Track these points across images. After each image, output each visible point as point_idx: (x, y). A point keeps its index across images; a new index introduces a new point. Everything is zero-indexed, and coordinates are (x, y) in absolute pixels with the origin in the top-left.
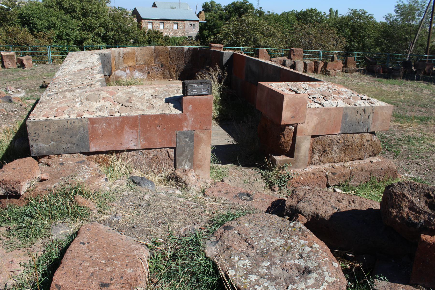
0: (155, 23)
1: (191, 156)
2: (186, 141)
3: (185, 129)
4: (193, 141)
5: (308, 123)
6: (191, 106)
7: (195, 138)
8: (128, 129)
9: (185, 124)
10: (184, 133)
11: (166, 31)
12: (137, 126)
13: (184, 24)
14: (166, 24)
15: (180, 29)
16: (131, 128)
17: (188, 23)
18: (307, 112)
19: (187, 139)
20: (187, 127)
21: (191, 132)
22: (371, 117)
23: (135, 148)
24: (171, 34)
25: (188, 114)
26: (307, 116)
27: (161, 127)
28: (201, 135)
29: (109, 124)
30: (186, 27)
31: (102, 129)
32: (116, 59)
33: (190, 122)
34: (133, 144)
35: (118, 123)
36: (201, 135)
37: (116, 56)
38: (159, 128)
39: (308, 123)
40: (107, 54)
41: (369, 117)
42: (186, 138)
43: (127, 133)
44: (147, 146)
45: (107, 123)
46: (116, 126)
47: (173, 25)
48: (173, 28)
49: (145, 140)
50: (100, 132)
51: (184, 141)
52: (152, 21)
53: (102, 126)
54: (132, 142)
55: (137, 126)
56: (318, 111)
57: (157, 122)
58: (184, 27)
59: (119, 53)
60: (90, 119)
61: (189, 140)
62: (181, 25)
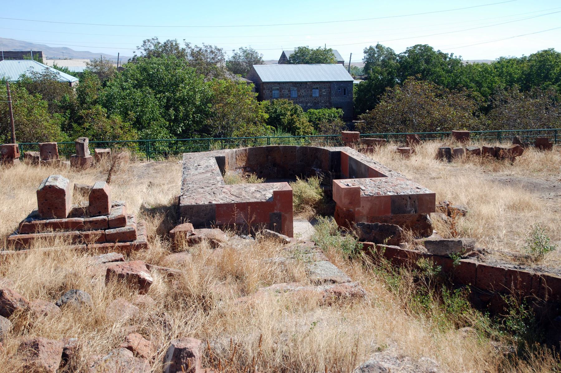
0: (283, 89)
3: (275, 211)
5: (363, 207)
9: (276, 208)
10: (275, 214)
14: (301, 89)
18: (362, 199)
19: (277, 218)
22: (416, 202)
25: (277, 202)
26: (361, 202)
28: (286, 215)
30: (332, 92)
36: (286, 215)
39: (363, 207)
41: (414, 202)
42: (276, 217)
47: (311, 91)
48: (311, 96)
56: (370, 199)
58: (330, 93)
62: (324, 90)
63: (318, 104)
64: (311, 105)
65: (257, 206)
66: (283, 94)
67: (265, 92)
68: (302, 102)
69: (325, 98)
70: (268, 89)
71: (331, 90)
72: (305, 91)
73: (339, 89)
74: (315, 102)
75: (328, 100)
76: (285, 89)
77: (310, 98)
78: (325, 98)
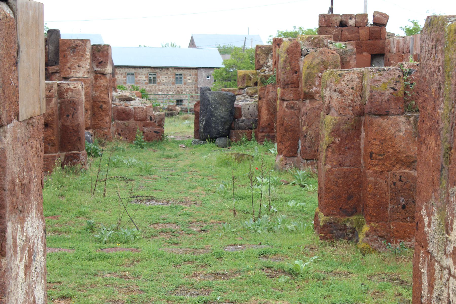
0: (139, 74)
11: (161, 88)
13: (196, 75)
14: (161, 75)
15: (189, 84)
17: (204, 74)
30: (199, 80)
52: (132, 71)
58: (196, 81)
62: (189, 78)
63: (182, 93)
66: (139, 80)
67: (118, 77)
68: (162, 90)
70: (121, 74)
71: (197, 78)
72: (166, 78)
73: (208, 77)
75: (193, 89)
76: (142, 74)
77: (172, 86)
78: (191, 86)
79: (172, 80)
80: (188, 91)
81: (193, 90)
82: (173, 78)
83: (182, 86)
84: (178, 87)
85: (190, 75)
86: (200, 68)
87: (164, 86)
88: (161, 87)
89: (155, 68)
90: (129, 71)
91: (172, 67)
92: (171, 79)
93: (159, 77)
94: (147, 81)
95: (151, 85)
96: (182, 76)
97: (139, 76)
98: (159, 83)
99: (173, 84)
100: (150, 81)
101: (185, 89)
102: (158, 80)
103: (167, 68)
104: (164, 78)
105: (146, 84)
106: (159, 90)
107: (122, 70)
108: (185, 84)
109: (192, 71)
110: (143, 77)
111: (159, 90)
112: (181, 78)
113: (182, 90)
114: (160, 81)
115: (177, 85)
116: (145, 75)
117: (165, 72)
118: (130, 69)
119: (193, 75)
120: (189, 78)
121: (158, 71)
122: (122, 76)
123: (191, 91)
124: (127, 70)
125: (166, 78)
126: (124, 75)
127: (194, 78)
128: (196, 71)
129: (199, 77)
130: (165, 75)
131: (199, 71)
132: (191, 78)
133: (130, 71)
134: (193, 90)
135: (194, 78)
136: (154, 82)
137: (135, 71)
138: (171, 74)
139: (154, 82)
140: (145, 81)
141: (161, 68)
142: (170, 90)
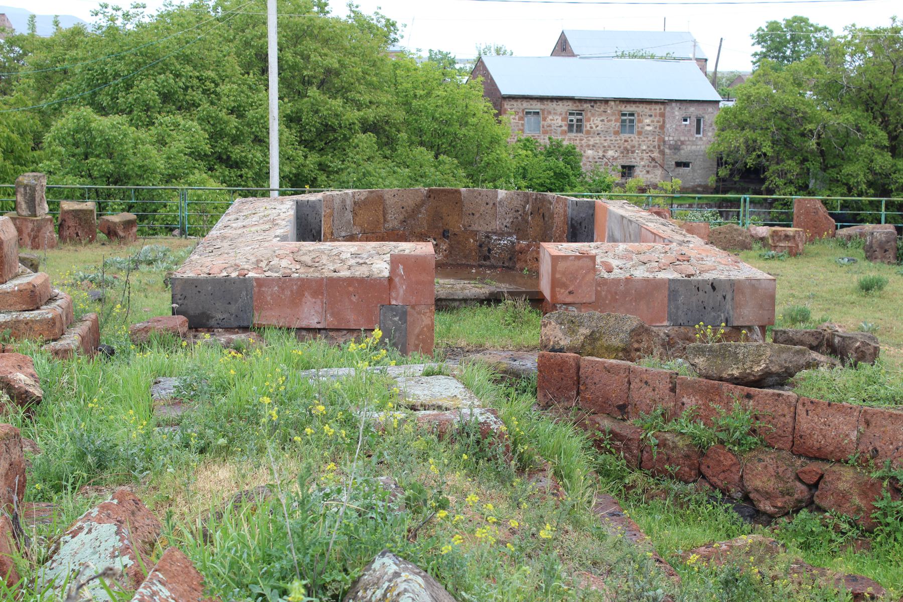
0: (549, 113)
1: (402, 345)
2: (395, 322)
4: (406, 322)
6: (401, 267)
7: (408, 318)
8: (309, 297)
11: (591, 143)
12: (322, 294)
13: (662, 115)
14: (593, 115)
15: (648, 133)
16: (313, 297)
17: (678, 112)
19: (396, 319)
20: (396, 300)
21: (403, 306)
23: (319, 326)
24: (610, 153)
27: (357, 297)
29: (282, 289)
30: (668, 126)
31: (271, 295)
32: (336, 215)
33: (401, 292)
34: (316, 321)
35: (295, 287)
37: (336, 207)
38: (354, 299)
40: (314, 202)
41: (724, 298)
42: (395, 316)
43: (308, 303)
44: (335, 325)
45: (279, 287)
46: (292, 291)
49: (332, 315)
50: (269, 298)
51: (391, 320)
52: (536, 106)
53: (272, 290)
54: (313, 317)
55: (322, 294)
57: (351, 289)
58: (662, 127)
59: (343, 201)
60: (257, 279)
61: (400, 320)
62: (648, 121)
63: (633, 152)
64: (616, 155)
65: (351, 289)
66: (550, 126)
68: (594, 146)
69: (651, 138)
71: (664, 122)
72: (602, 121)
73: (685, 120)
74: (626, 149)
75: (656, 143)
76: (555, 114)
77: (613, 138)
78: (651, 138)
79: (615, 125)
80: (644, 148)
81: (654, 147)
82: (616, 121)
83: (634, 138)
84: (626, 141)
85: (651, 116)
86: (671, 101)
87: (598, 138)
88: (592, 139)
89: (581, 101)
90: (529, 107)
91: (615, 100)
92: (613, 124)
93: (588, 120)
94: (565, 128)
95: (572, 135)
96: (635, 118)
97: (550, 117)
98: (588, 132)
99: (616, 133)
100: (570, 127)
101: (640, 145)
102: (587, 126)
103: (606, 101)
104: (598, 122)
105: (564, 133)
106: (588, 146)
107: (517, 105)
108: (640, 133)
109: (654, 107)
110: (557, 119)
111: (588, 146)
112: (632, 121)
113: (634, 147)
114: (591, 128)
115: (626, 136)
116: (561, 114)
117: (602, 109)
118: (531, 102)
119: (655, 116)
120: (648, 122)
121: (587, 106)
122: (517, 117)
123: (651, 148)
124: (525, 105)
125: (602, 121)
126: (521, 114)
127: (658, 122)
128: (662, 107)
129: (667, 120)
130: (600, 115)
131: (668, 108)
132: (653, 121)
133: (532, 107)
134: (654, 147)
135: (658, 122)
136: (579, 129)
137: (543, 107)
138: (613, 114)
139: (579, 129)
140: (561, 126)
141: (594, 101)
142: (609, 147)
